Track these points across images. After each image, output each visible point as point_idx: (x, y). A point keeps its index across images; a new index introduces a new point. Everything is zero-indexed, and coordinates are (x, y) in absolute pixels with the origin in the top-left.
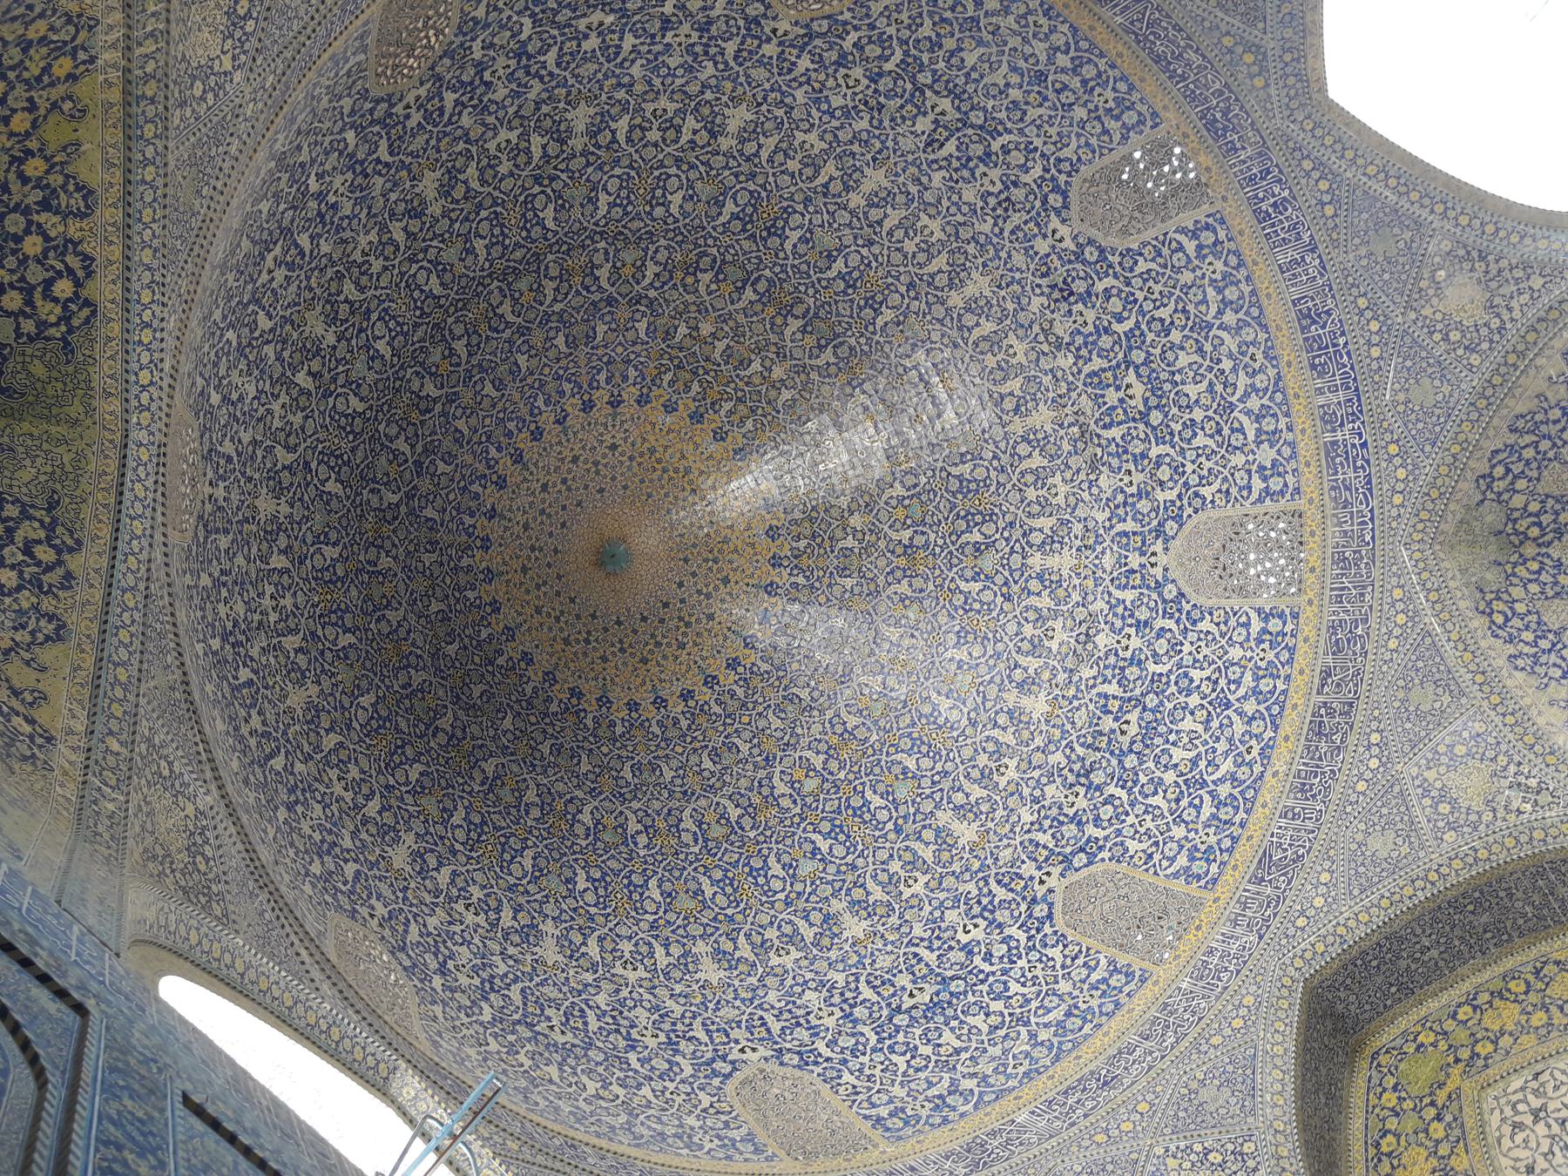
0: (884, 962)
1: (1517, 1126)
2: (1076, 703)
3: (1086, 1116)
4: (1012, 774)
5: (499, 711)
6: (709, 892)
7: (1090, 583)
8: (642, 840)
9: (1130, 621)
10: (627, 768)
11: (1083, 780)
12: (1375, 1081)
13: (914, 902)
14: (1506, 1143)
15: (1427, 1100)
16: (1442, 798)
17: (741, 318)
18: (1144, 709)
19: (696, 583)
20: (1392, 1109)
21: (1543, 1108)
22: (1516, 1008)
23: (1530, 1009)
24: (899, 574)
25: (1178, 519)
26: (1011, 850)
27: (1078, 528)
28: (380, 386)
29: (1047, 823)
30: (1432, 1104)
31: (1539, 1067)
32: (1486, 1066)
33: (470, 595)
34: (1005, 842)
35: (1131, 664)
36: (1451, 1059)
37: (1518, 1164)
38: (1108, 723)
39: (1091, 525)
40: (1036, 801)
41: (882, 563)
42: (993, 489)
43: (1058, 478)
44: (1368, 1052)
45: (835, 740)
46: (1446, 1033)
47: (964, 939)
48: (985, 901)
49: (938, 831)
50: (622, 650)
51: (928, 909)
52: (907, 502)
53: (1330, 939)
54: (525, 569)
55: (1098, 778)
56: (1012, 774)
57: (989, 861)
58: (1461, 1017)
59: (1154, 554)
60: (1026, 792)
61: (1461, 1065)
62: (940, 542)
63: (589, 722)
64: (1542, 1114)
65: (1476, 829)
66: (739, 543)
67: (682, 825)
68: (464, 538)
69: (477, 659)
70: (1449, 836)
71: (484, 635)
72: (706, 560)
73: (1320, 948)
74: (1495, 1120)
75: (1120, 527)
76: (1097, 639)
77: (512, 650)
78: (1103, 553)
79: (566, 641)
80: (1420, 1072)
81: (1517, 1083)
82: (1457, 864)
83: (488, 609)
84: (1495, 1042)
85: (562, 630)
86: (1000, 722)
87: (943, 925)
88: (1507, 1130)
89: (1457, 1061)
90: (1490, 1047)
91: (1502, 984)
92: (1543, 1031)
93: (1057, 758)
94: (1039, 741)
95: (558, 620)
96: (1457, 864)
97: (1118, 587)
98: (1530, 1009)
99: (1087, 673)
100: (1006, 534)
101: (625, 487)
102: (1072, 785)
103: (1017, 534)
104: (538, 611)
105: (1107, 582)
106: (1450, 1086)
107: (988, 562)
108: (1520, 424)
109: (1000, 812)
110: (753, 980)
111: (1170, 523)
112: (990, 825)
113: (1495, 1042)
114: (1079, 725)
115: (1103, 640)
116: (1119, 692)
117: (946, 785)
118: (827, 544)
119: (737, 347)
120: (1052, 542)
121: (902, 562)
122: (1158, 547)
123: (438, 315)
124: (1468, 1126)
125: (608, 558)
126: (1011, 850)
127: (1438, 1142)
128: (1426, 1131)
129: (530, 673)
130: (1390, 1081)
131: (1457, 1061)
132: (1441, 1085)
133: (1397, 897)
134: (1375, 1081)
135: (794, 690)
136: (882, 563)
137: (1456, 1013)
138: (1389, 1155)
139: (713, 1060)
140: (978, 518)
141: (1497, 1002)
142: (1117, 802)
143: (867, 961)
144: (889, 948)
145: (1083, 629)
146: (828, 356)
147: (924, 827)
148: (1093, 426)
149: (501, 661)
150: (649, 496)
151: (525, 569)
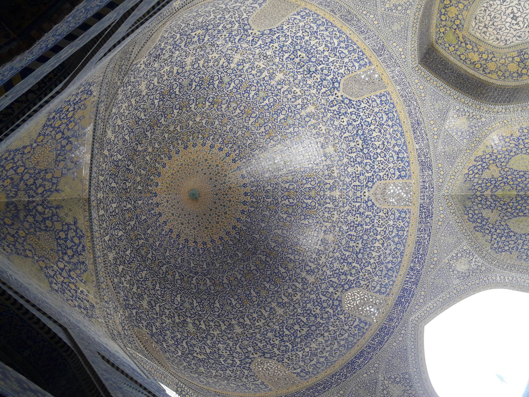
0: (344, 146)
1: (484, 33)
2: (285, 66)
3: (426, 135)
4: (298, 90)
5: (254, 239)
6: (310, 186)
7: (248, 52)
8: (291, 200)
9: (268, 44)
10: (267, 200)
11: (311, 73)
12: (444, 48)
13: (327, 131)
14: (487, 38)
15: (460, 43)
16: (396, 7)
17: (136, 167)
18: (299, 50)
19: (205, 169)
20: (455, 50)
21: (485, 25)
22: (453, 7)
23: (456, 5)
24: (219, 107)
25: (245, 25)
26: (322, 100)
27: (229, 52)
28: (186, 295)
29: (319, 87)
30: (461, 42)
31: (474, 16)
32: (463, 26)
33: (221, 248)
34: (319, 100)
35: (282, 48)
36: (454, 30)
37: (494, 40)
38: (297, 60)
39: (231, 48)
40: (310, 87)
41: (214, 112)
42: (204, 76)
43: (210, 56)
44: (435, 43)
45: (267, 136)
46: (445, 26)
47: (345, 123)
48: (336, 113)
49: (307, 116)
50: (226, 195)
51: (331, 128)
52: (197, 103)
53: (413, 53)
54: (206, 228)
55: (313, 69)
56: (298, 90)
57: (323, 106)
58: (444, 19)
59: (251, 33)
60: (306, 88)
61: (457, 29)
62: (214, 93)
63: (252, 209)
64: (487, 26)
65: (412, 5)
66: (195, 156)
67: (287, 187)
68: (206, 252)
69: (240, 245)
70: (408, 12)
71: (231, 243)
72: (199, 166)
73: (413, 56)
74: (478, 35)
75: (236, 41)
76: (268, 54)
77: (233, 233)
78: (241, 46)
79: (226, 213)
80: (450, 37)
81: (474, 24)
82: (417, 14)
83: (223, 241)
84: (458, 19)
85: (222, 215)
86: (280, 88)
87: (338, 126)
88: (483, 35)
89: (455, 29)
90: (459, 21)
91: (443, 4)
92: (465, 8)
93: (299, 77)
94: (291, 80)
95: (219, 216)
96: (417, 14)
97: (255, 44)
98: (456, 5)
99: (277, 60)
100: (220, 73)
101: (176, 194)
102: (311, 76)
103: (221, 70)
104: (218, 223)
105: (251, 47)
106: (461, 36)
107: (226, 79)
108: (478, 159)
109: (309, 98)
110: (341, 183)
111: (246, 27)
112: (312, 101)
113: (458, 19)
114: (292, 67)
115: (269, 53)
116: (289, 54)
117: (293, 109)
118: (202, 128)
119: (143, 166)
120: (229, 61)
121: (216, 106)
122: (250, 31)
123: (162, 282)
124: (475, 41)
125: (194, 197)
126: (322, 100)
127: (472, 49)
128: (467, 49)
129: (239, 227)
130: (447, 45)
131: (455, 29)
132: (459, 37)
133: (414, 32)
134: (444, 48)
135: (247, 144)
136: (214, 112)
137: (442, 20)
138: (466, 59)
139: (367, 205)
140: (211, 81)
141: (447, 10)
142: (324, 68)
143: (342, 151)
144: (340, 143)
145: (262, 57)
146: (149, 134)
147: (304, 119)
148: (201, 45)
149: (238, 237)
150: (178, 185)
151: (206, 228)
